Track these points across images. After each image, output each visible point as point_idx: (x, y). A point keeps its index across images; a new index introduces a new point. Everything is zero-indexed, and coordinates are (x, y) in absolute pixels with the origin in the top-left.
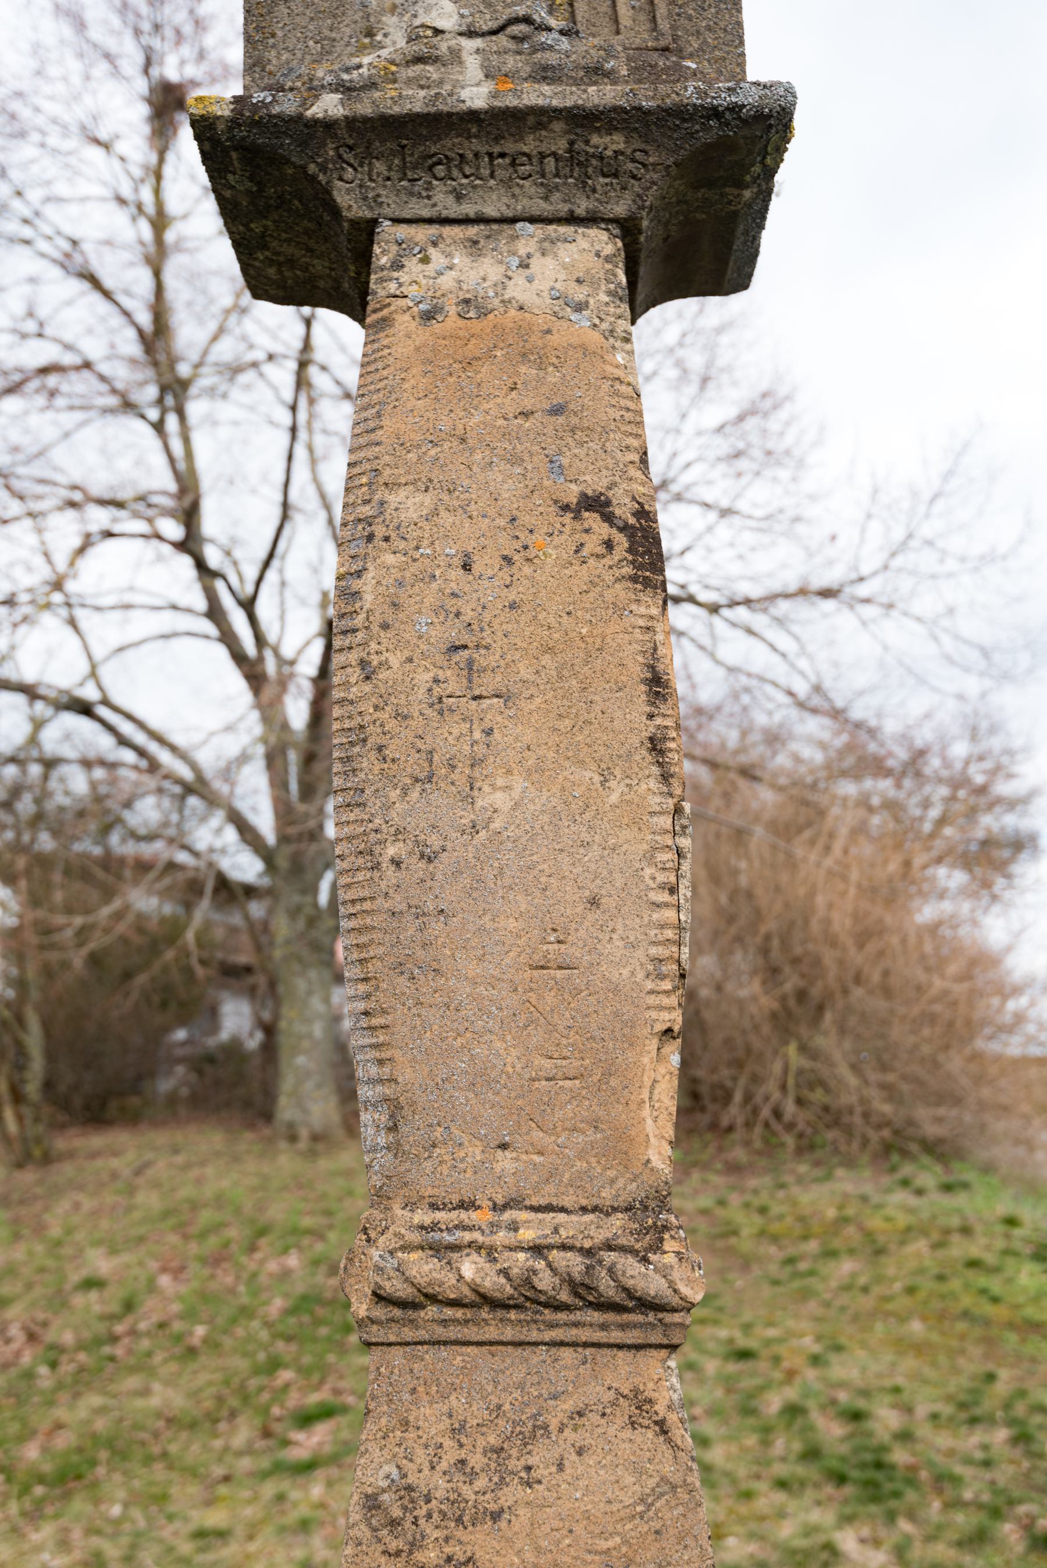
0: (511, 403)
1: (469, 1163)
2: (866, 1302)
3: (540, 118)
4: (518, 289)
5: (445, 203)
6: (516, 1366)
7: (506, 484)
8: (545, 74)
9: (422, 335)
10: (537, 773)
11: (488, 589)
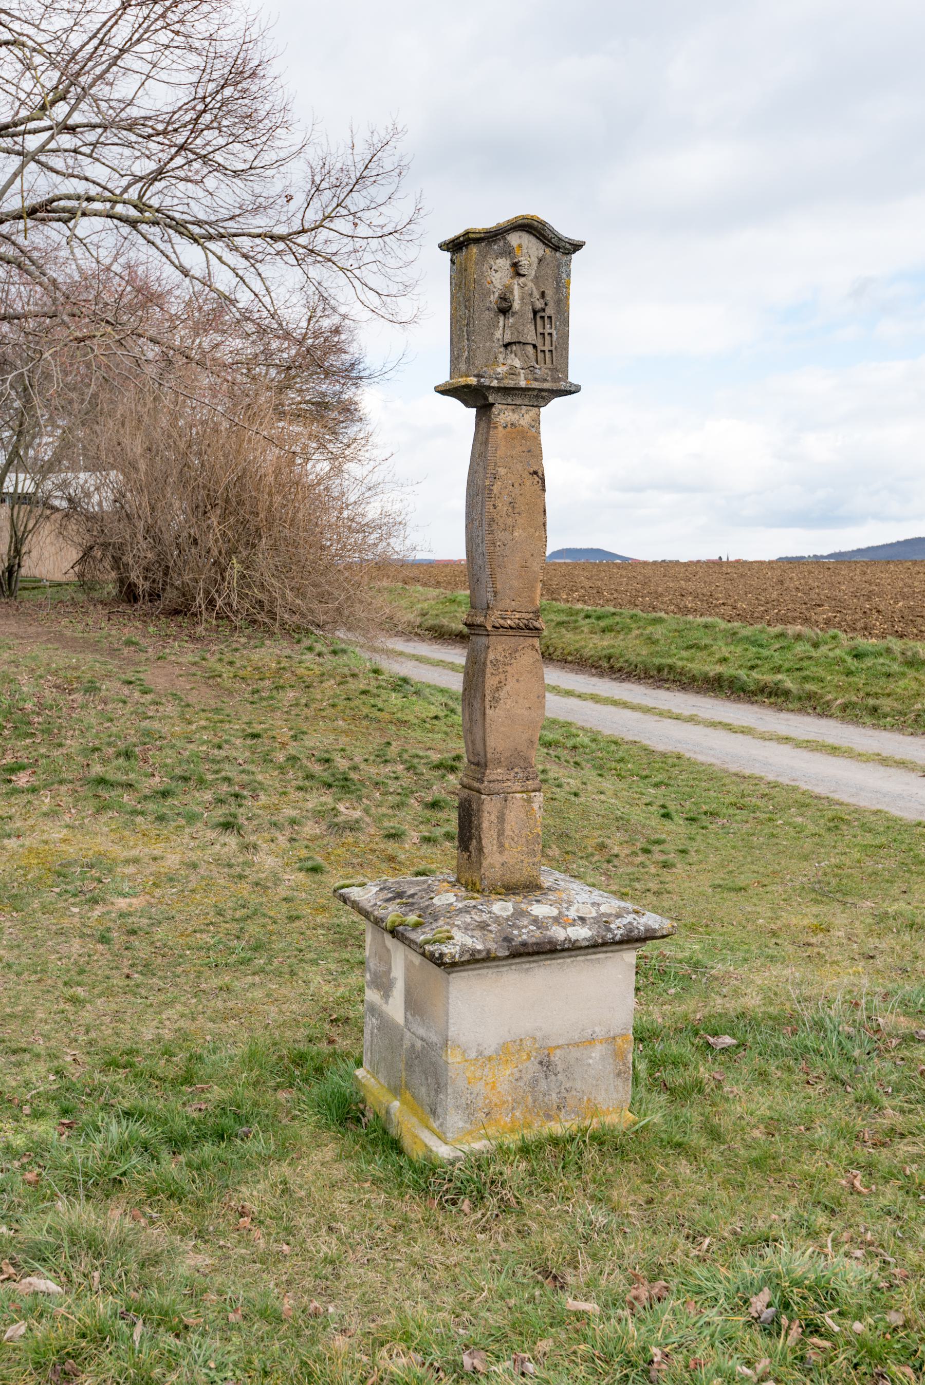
0: (521, 449)
1: (507, 603)
2: (310, 712)
3: (534, 389)
4: (522, 422)
5: (509, 401)
6: (513, 639)
7: (519, 467)
8: (536, 380)
9: (504, 432)
10: (524, 529)
11: (517, 490)
